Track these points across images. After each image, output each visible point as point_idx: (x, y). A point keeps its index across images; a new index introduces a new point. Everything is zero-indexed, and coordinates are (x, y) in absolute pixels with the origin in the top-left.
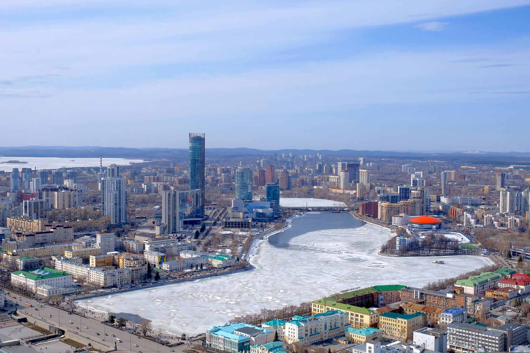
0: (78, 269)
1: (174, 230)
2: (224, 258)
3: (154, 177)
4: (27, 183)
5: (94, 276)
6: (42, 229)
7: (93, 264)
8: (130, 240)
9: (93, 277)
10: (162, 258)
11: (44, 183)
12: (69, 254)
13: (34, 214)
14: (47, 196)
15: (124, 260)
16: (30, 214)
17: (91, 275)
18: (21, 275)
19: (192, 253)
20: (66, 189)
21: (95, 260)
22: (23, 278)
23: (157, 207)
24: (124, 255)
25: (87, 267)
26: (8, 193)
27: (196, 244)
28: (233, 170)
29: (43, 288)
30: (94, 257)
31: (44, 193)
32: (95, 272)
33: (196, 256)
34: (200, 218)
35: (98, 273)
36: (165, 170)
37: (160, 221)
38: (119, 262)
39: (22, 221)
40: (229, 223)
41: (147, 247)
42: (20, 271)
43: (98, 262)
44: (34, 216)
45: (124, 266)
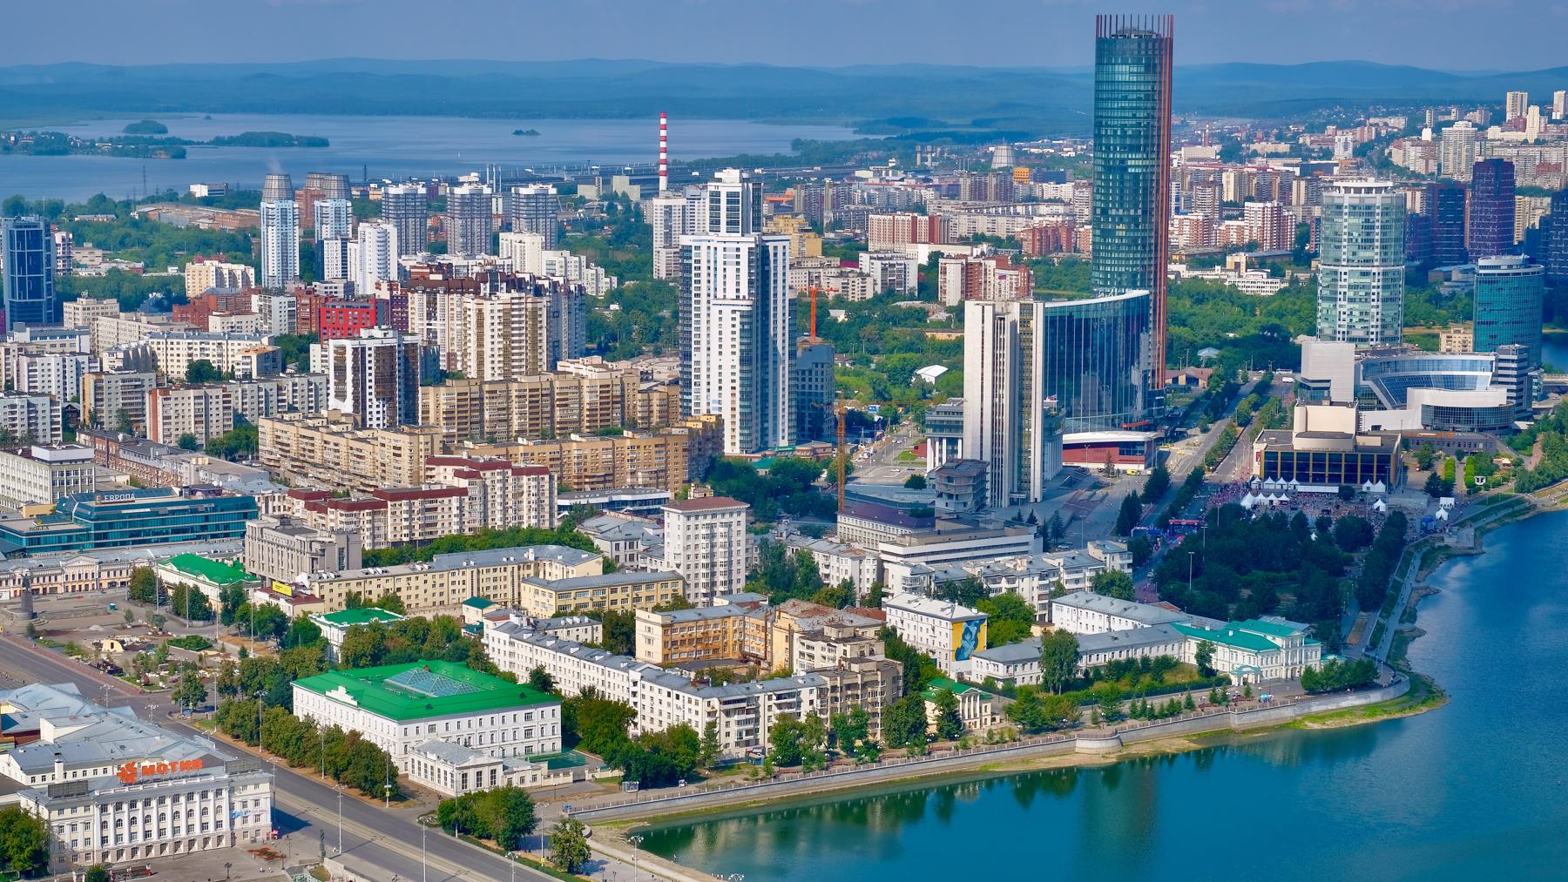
0: (583, 671)
1: (1020, 490)
2: (1269, 638)
3: (914, 219)
4: (332, 252)
5: (657, 707)
6: (415, 476)
7: (649, 648)
8: (817, 534)
9: (656, 711)
10: (967, 631)
11: (411, 248)
12: (541, 598)
13: (375, 402)
14: (431, 315)
15: (796, 636)
16: (360, 403)
17: (647, 702)
18: (340, 693)
19: (1112, 610)
20: (515, 283)
21: (658, 631)
22: (349, 709)
23: (938, 370)
24: (792, 611)
25: (632, 666)
26: (255, 298)
27: (1129, 565)
28: (1303, 184)
29: (434, 757)
30: (657, 618)
31: (417, 301)
32: (665, 690)
33: (1130, 627)
34: (1140, 429)
35: (678, 697)
36: (965, 183)
37: (952, 442)
38: (768, 642)
39: (327, 438)
40: (1287, 456)
41: (897, 575)
42: (331, 676)
43: (674, 643)
44: (374, 410)
45: (796, 667)
